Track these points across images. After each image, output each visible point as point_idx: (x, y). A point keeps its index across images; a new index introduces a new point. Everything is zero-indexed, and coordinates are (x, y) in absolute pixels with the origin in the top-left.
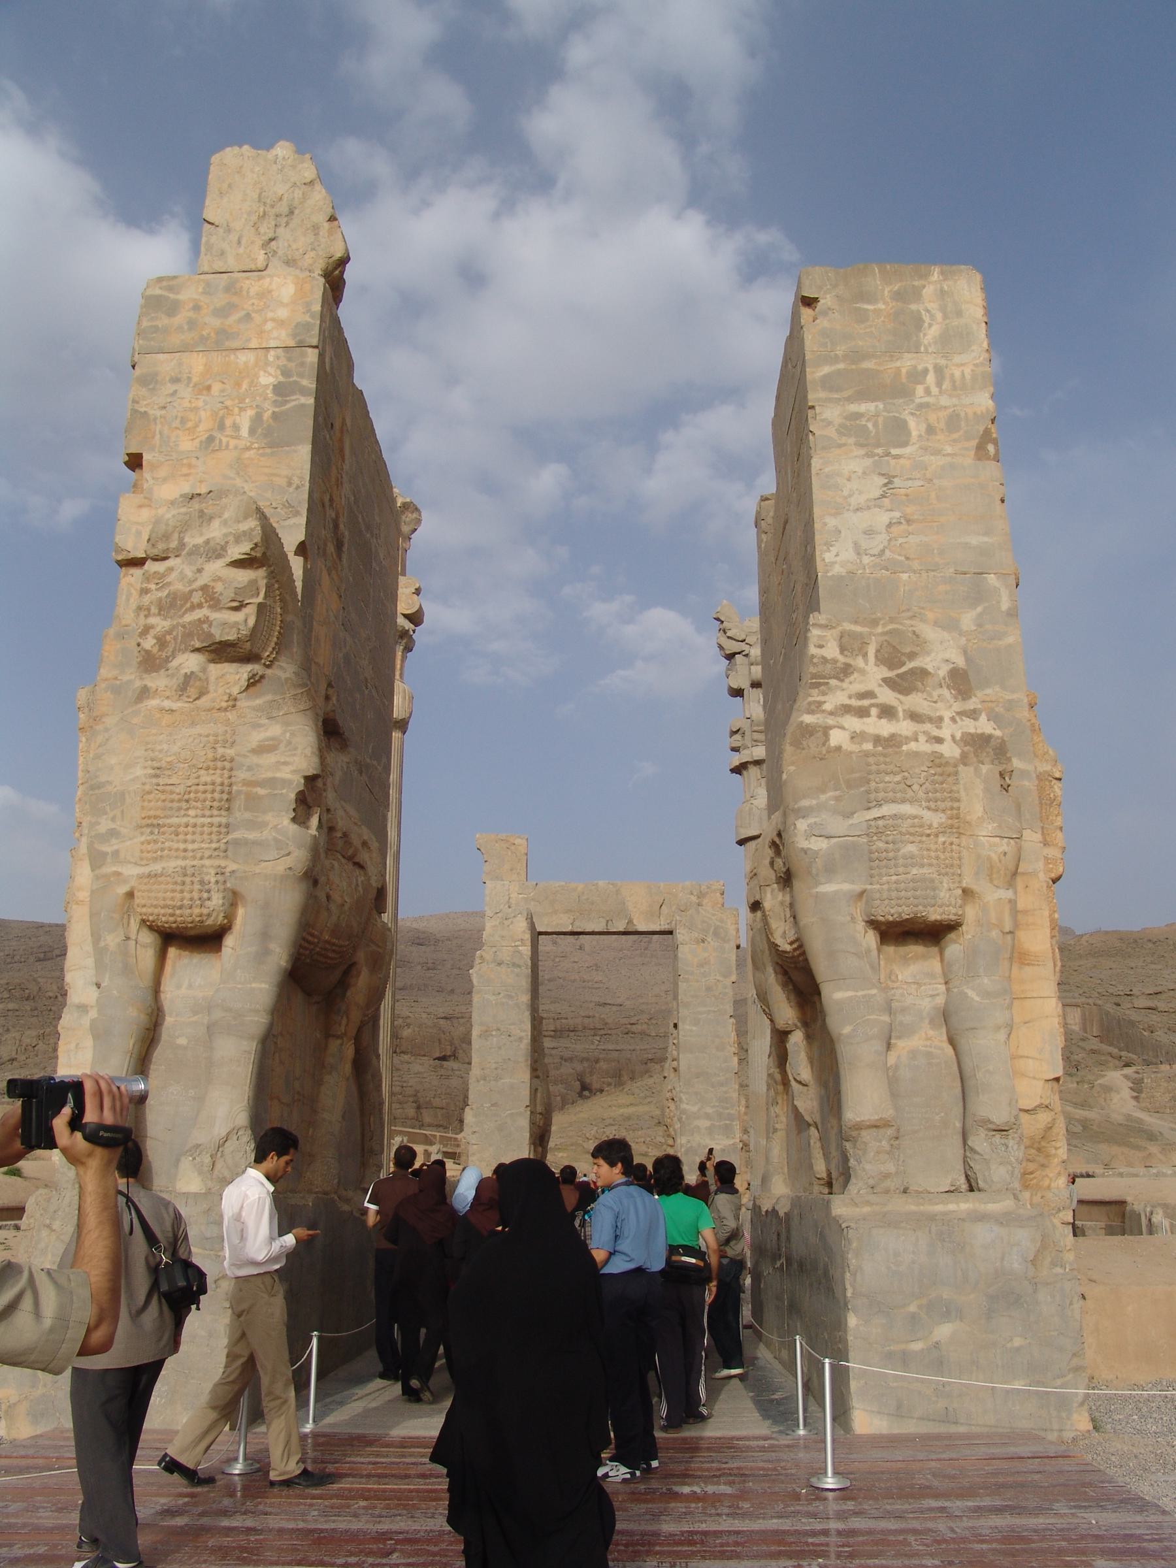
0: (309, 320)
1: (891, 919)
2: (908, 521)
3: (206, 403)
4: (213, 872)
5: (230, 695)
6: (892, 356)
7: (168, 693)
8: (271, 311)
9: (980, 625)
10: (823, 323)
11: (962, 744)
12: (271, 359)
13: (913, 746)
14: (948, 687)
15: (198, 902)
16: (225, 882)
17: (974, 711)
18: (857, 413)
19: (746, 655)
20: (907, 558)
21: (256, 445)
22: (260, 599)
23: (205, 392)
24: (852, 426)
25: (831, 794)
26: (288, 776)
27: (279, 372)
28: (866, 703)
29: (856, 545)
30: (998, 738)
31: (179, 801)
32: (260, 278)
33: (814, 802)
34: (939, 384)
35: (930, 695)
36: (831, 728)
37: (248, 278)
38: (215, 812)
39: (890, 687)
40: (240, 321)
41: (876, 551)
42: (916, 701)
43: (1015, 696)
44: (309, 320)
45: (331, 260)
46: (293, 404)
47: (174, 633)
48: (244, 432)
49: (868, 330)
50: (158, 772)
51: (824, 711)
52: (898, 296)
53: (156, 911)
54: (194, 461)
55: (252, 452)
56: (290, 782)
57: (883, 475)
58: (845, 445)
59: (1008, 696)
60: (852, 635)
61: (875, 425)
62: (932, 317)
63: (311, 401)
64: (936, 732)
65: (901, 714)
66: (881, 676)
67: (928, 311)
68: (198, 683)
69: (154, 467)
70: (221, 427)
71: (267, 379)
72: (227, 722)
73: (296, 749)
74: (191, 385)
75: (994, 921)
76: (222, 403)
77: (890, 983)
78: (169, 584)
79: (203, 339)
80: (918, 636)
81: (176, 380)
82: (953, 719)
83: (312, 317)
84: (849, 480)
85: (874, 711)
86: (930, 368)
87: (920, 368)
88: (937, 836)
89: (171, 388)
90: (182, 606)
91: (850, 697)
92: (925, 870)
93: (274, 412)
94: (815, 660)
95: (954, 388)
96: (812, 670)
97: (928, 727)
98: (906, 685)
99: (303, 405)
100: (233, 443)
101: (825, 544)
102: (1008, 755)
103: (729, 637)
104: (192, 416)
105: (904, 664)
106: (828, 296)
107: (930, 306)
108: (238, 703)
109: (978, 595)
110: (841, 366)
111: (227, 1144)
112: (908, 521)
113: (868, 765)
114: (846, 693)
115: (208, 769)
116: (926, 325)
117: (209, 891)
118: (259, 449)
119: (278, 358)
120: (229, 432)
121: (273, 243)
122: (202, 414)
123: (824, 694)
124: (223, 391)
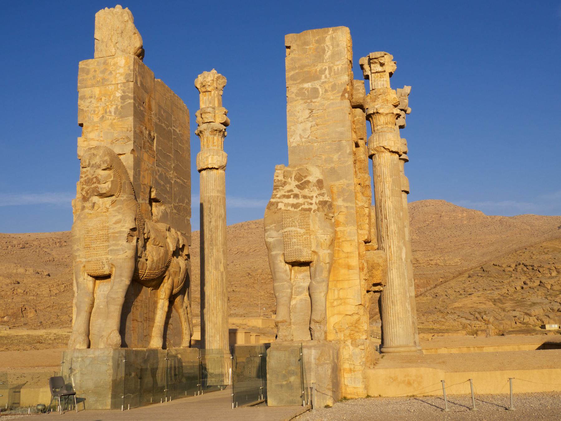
0: (130, 72)
1: (290, 261)
2: (317, 125)
3: (100, 104)
4: (105, 259)
5: (106, 208)
6: (314, 65)
7: (90, 208)
8: (118, 70)
9: (339, 159)
10: (292, 55)
11: (318, 204)
12: (119, 87)
13: (303, 206)
14: (316, 186)
15: (101, 268)
16: (109, 262)
17: (323, 193)
18: (302, 88)
20: (316, 138)
21: (117, 118)
22: (112, 179)
23: (100, 101)
24: (300, 93)
25: (273, 225)
26: (124, 230)
27: (122, 92)
28: (290, 194)
29: (300, 135)
30: (329, 202)
31: (94, 240)
32: (114, 58)
33: (269, 228)
34: (330, 74)
35: (310, 189)
36: (279, 202)
37: (110, 59)
38: (104, 242)
39: (297, 188)
40: (109, 74)
41: (306, 137)
42: (306, 192)
43: (350, 182)
44: (130, 72)
45: (136, 49)
46: (127, 103)
48: (113, 114)
49: (307, 56)
50: (88, 232)
51: (277, 197)
52: (318, 42)
53: (91, 271)
54: (98, 125)
55: (116, 120)
56: (125, 231)
57: (310, 109)
58: (298, 100)
59: (347, 182)
60: (287, 171)
61: (308, 92)
62: (329, 48)
63: (132, 101)
64: (310, 201)
65: (300, 197)
66: (295, 184)
67: (327, 46)
68: (97, 205)
69: (87, 127)
70: (106, 112)
71: (119, 94)
72: (107, 216)
73: (126, 222)
74: (96, 98)
75: (321, 260)
76: (105, 104)
77: (296, 280)
78: (87, 175)
79: (98, 82)
80: (308, 170)
81: (91, 97)
82: (316, 197)
83: (131, 71)
84: (298, 112)
85: (292, 196)
86: (327, 67)
87: (324, 68)
88: (302, 236)
89: (89, 100)
91: (285, 192)
92: (299, 247)
93: (121, 106)
94: (276, 181)
95: (335, 74)
96: (275, 184)
97: (309, 200)
98: (303, 186)
99: (130, 103)
100: (110, 117)
101: (291, 136)
102: (333, 207)
104: (97, 109)
105: (303, 180)
106: (294, 45)
108: (109, 210)
109: (339, 148)
110: (297, 71)
111: (111, 335)
112: (317, 125)
113: (283, 216)
114: (284, 191)
115: (101, 230)
116: (326, 51)
117: (104, 265)
118: (117, 119)
119: (121, 86)
120: (108, 114)
121: (117, 44)
122: (100, 108)
123: (277, 192)
124: (105, 100)
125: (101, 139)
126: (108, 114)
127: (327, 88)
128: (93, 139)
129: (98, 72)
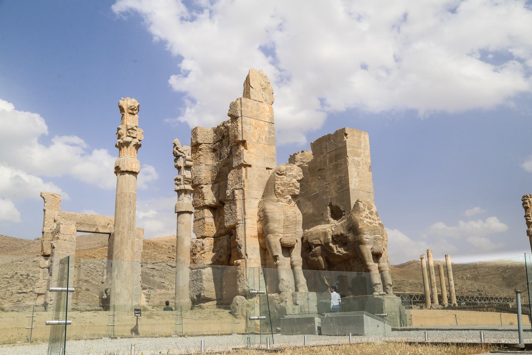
19: (183, 157)
34: (364, 156)
47: (286, 190)
48: (264, 140)
53: (288, 243)
64: (375, 222)
81: (250, 125)
85: (368, 218)
90: (287, 186)
97: (375, 221)
100: (262, 142)
103: (180, 151)
107: (363, 139)
110: (351, 149)
112: (361, 181)
124: (259, 129)
125: (258, 155)
126: (261, 139)
127: (363, 162)
128: (253, 153)
129: (253, 109)
